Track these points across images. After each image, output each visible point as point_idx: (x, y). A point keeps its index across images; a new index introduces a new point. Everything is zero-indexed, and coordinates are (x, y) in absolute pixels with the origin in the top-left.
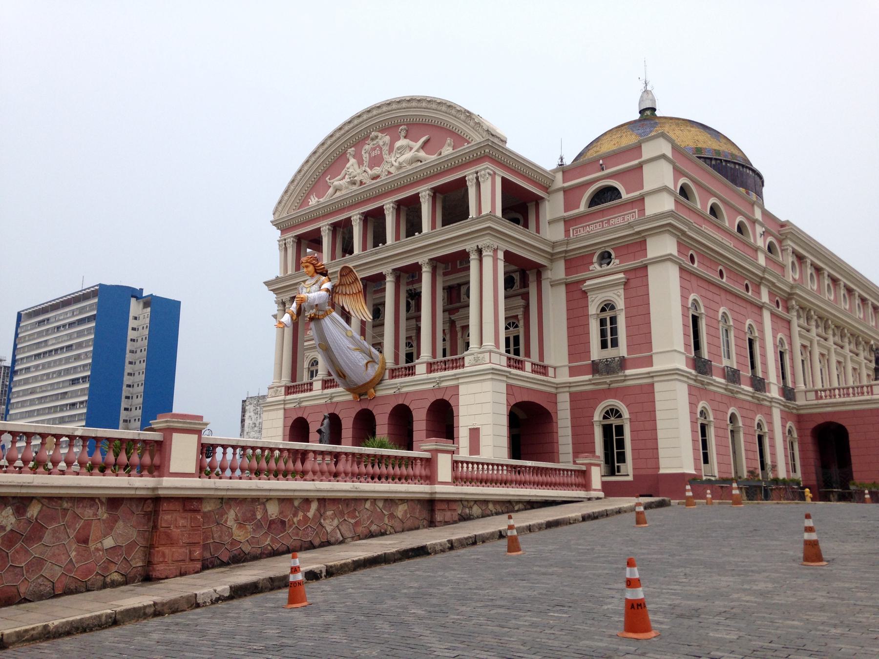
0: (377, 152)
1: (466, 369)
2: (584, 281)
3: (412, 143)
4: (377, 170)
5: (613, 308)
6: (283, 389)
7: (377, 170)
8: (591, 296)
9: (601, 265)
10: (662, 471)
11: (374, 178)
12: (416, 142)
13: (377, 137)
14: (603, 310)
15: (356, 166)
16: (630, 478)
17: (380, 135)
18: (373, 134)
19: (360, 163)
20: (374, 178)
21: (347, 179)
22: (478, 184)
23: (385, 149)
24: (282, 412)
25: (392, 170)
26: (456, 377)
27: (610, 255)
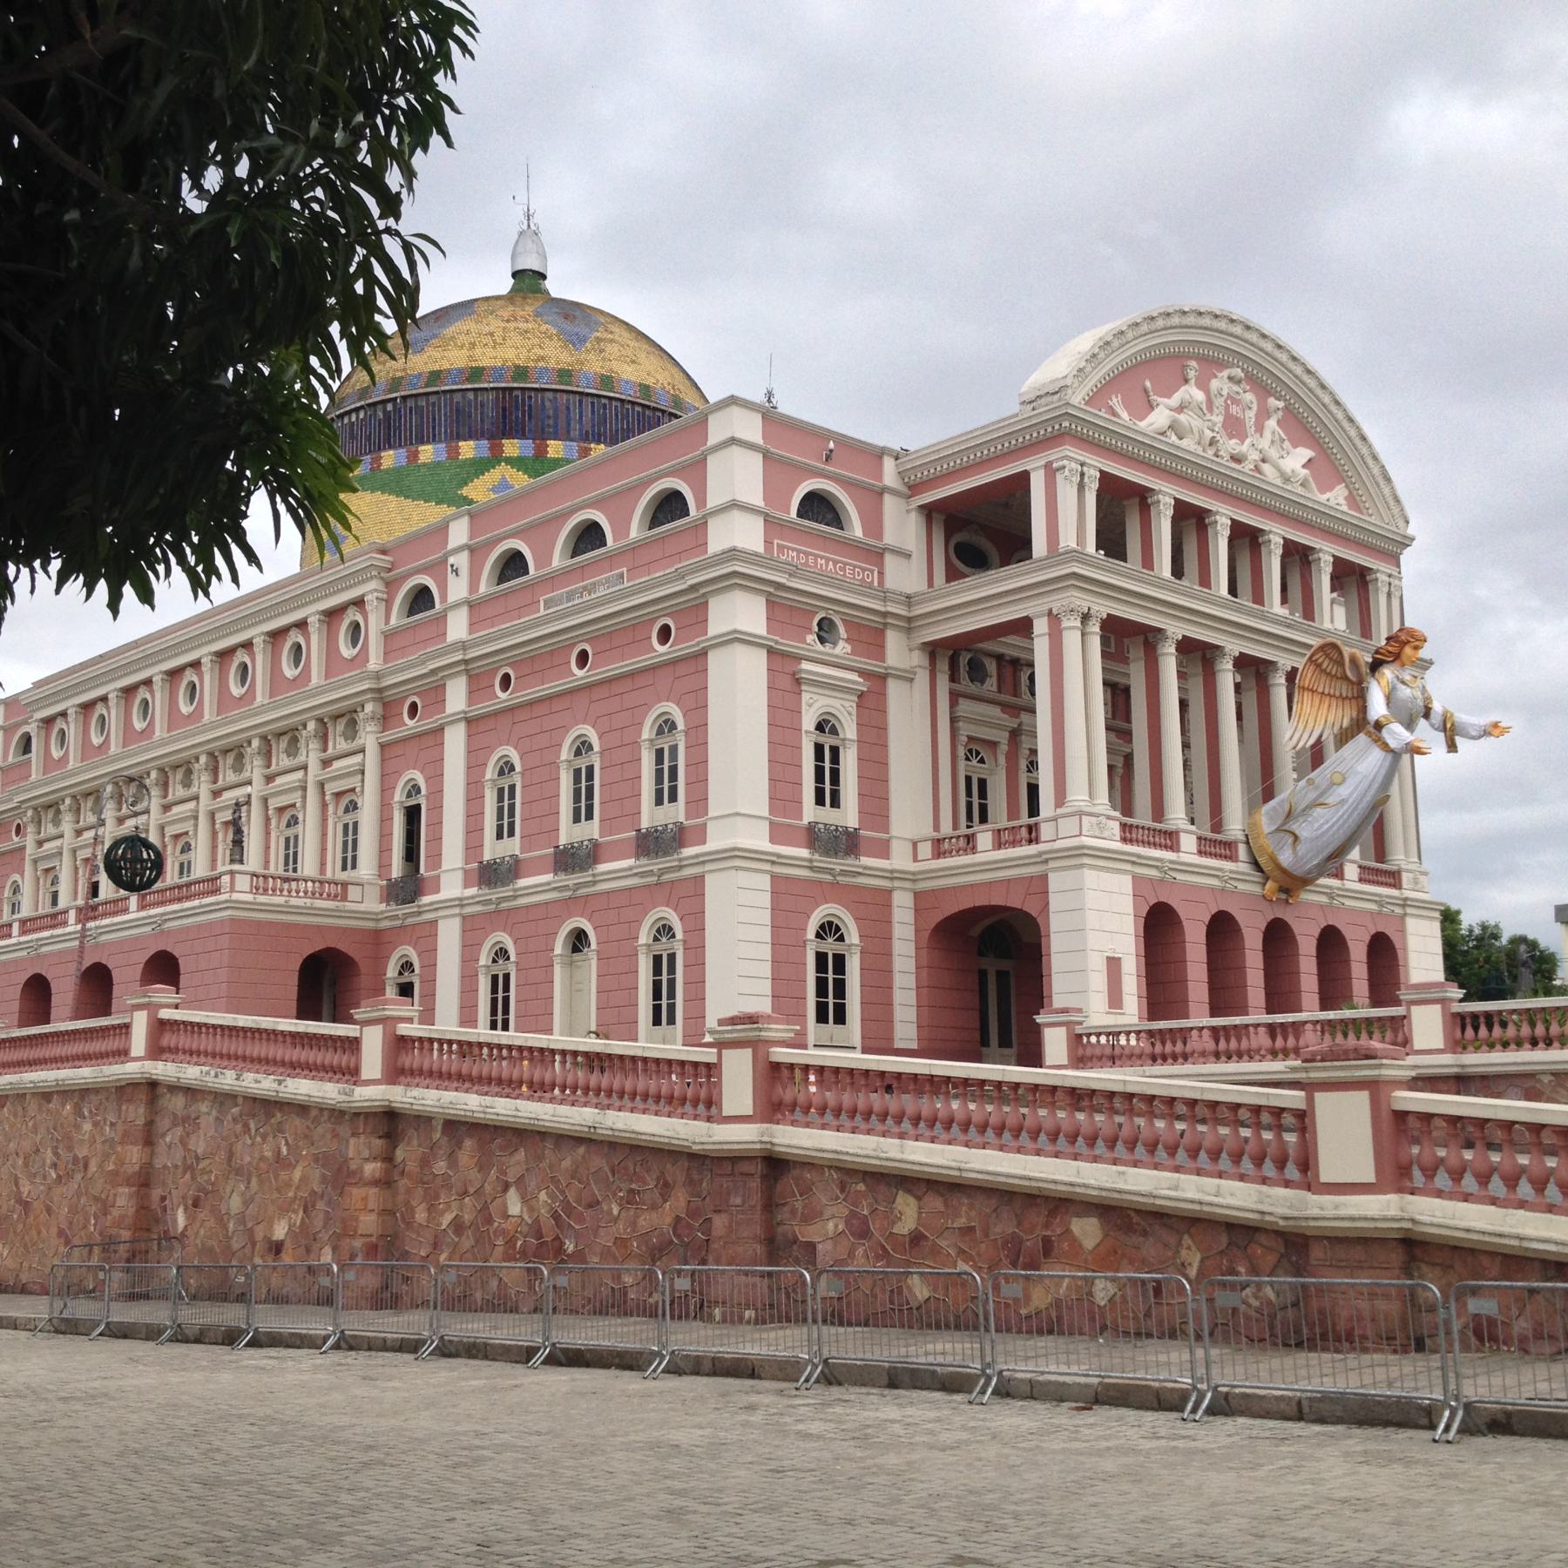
4: (1232, 446)
6: (1116, 826)
7: (1232, 446)
13: (1239, 382)
17: (1243, 385)
18: (1238, 372)
23: (1251, 415)
24: (1128, 880)
25: (1266, 467)
26: (1405, 903)
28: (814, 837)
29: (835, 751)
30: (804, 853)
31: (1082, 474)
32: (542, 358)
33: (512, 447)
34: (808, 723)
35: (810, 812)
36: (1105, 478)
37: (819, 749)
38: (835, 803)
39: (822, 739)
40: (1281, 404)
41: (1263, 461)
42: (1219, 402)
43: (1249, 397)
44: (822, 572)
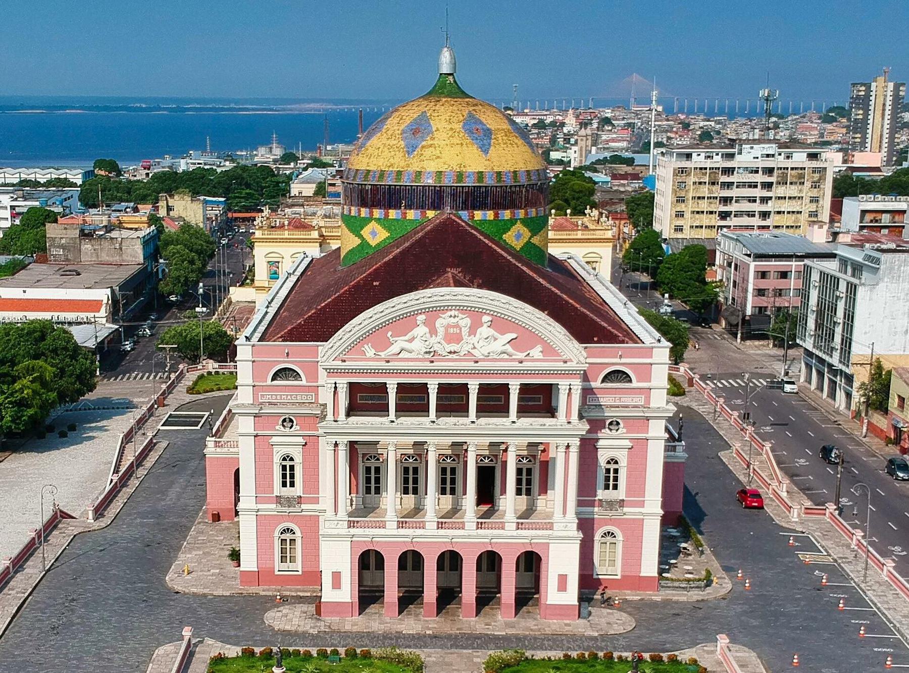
0: (457, 331)
1: (556, 533)
2: (597, 440)
3: (497, 335)
5: (616, 462)
8: (600, 453)
9: (611, 430)
10: (642, 574)
11: (450, 353)
12: (503, 333)
14: (609, 462)
15: (428, 335)
16: (619, 577)
17: (460, 315)
19: (433, 331)
20: (450, 353)
21: (418, 346)
22: (569, 394)
23: (465, 331)
26: (549, 537)
27: (618, 424)
28: (279, 499)
29: (292, 468)
30: (273, 506)
31: (336, 388)
32: (392, 165)
33: (378, 213)
34: (277, 460)
35: (278, 489)
36: (351, 385)
37: (284, 468)
38: (292, 485)
39: (284, 463)
40: (490, 318)
41: (475, 348)
42: (441, 331)
43: (465, 322)
44: (286, 398)
